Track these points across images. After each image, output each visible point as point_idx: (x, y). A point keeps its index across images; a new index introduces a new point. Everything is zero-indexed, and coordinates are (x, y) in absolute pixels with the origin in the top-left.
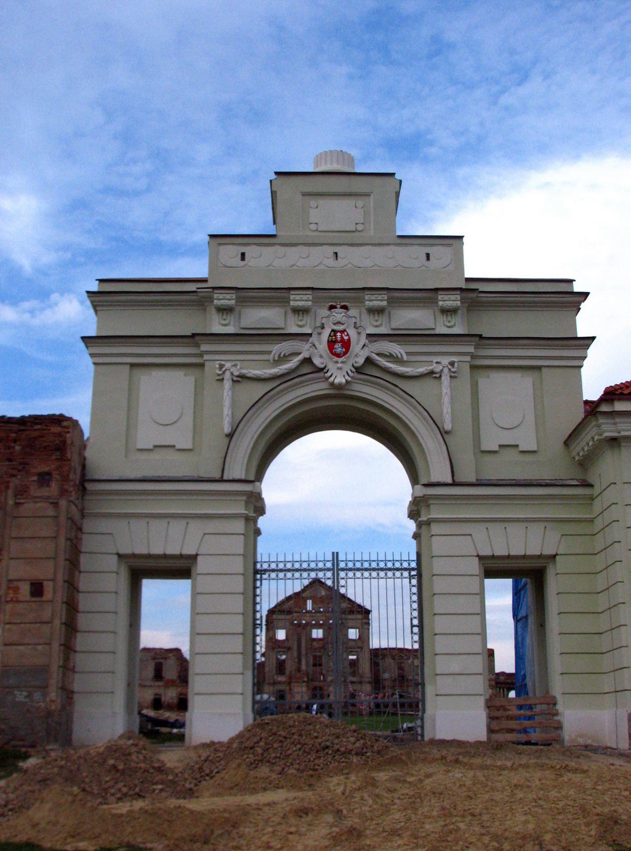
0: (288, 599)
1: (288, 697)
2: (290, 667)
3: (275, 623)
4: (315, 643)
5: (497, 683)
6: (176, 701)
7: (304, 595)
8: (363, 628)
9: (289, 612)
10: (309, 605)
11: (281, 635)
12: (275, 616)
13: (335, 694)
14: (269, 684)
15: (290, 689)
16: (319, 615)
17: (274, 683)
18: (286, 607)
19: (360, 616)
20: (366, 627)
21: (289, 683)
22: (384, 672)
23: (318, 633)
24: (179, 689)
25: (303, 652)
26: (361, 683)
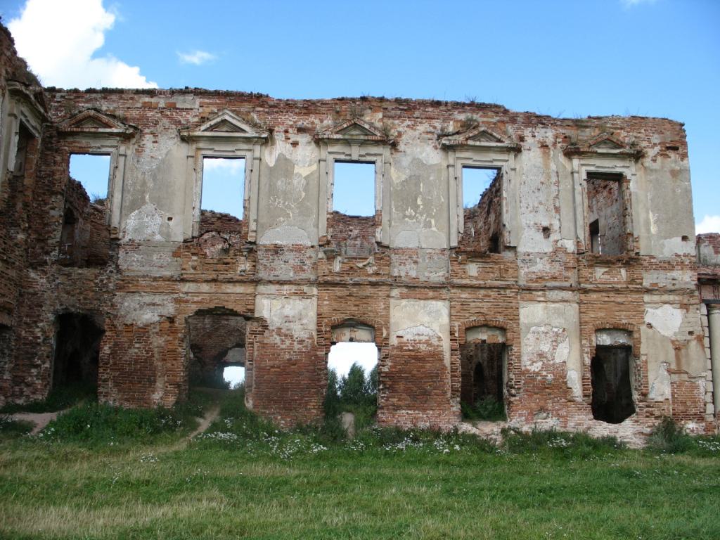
5: (703, 282)
22: (136, 204)
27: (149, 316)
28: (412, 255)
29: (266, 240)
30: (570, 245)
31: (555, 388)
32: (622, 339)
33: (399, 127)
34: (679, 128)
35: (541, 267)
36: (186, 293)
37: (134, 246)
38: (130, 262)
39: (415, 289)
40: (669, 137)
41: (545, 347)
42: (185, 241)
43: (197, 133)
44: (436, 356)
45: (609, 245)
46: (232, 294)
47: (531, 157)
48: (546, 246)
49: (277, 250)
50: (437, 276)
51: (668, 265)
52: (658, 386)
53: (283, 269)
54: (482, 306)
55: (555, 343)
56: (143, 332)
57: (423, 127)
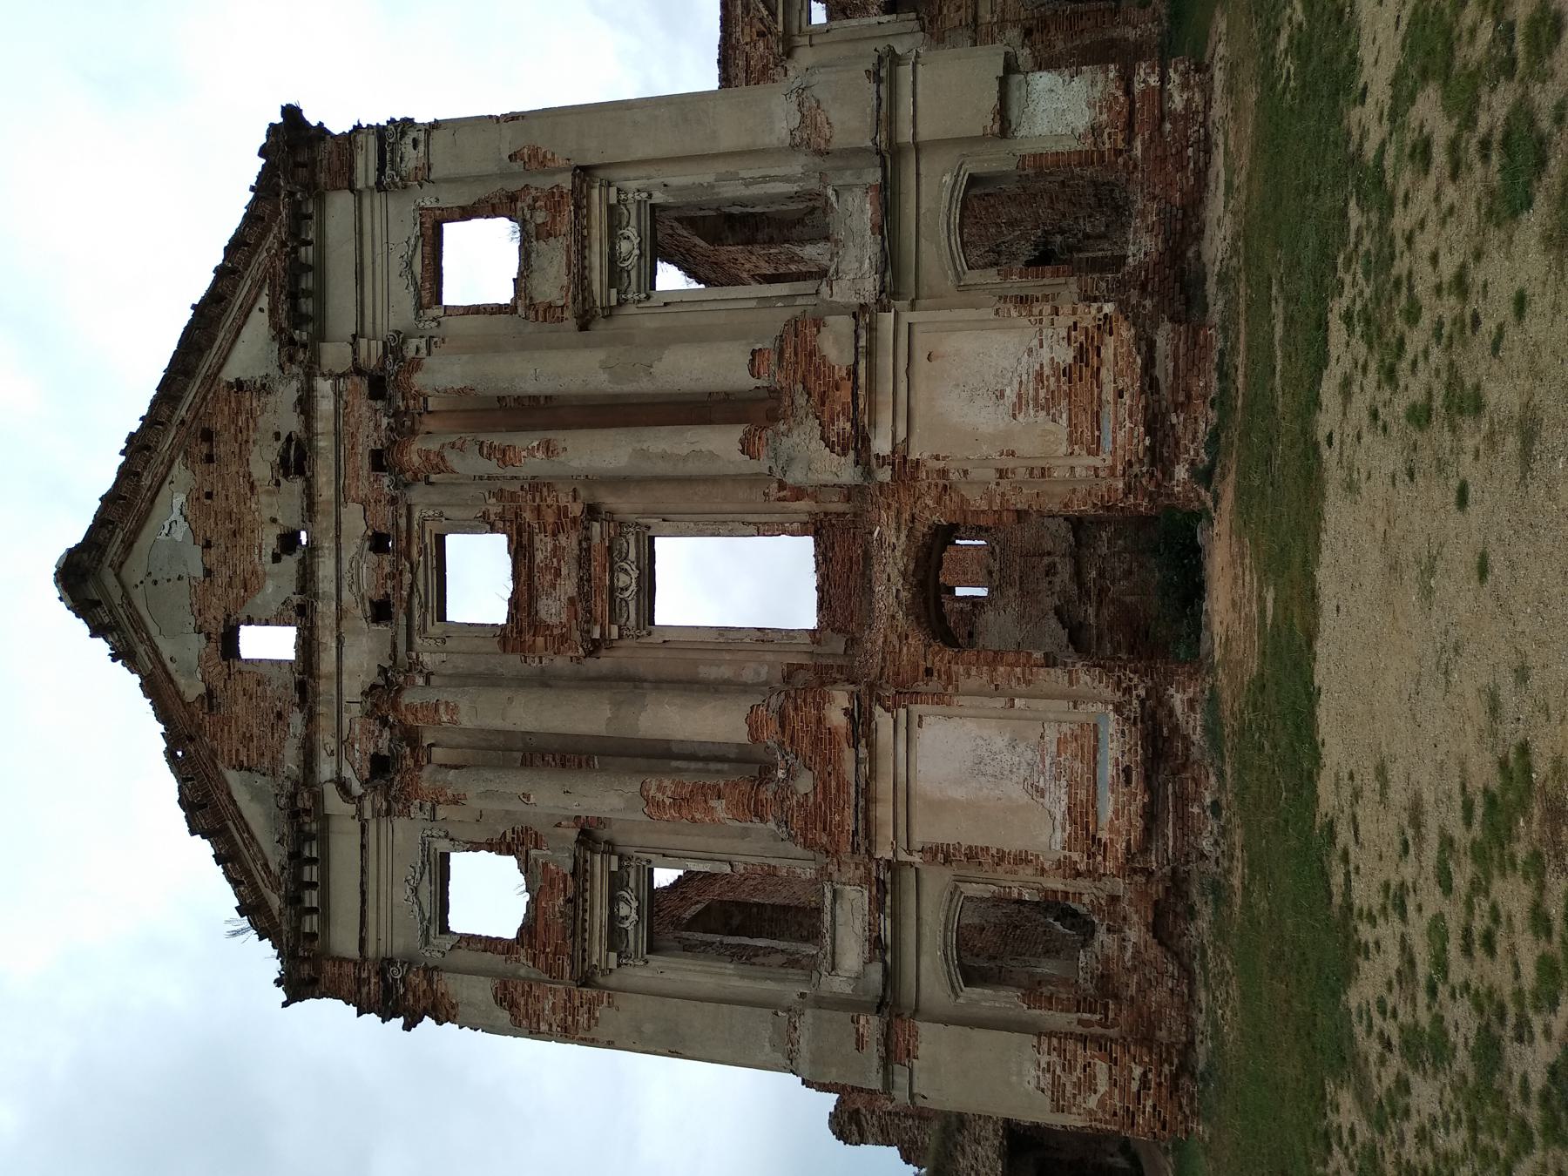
0: (205, 809)
3: (397, 934)
4: (552, 609)
7: (192, 689)
8: (425, 175)
9: (303, 820)
10: (270, 643)
11: (488, 895)
12: (344, 940)
14: (894, 1053)
15: (942, 855)
16: (326, 569)
17: (891, 1005)
19: (340, 206)
20: (411, 158)
23: (479, 579)
25: (585, 716)
26: (890, 156)
36: (992, 12)
42: (923, 30)
43: (781, 28)
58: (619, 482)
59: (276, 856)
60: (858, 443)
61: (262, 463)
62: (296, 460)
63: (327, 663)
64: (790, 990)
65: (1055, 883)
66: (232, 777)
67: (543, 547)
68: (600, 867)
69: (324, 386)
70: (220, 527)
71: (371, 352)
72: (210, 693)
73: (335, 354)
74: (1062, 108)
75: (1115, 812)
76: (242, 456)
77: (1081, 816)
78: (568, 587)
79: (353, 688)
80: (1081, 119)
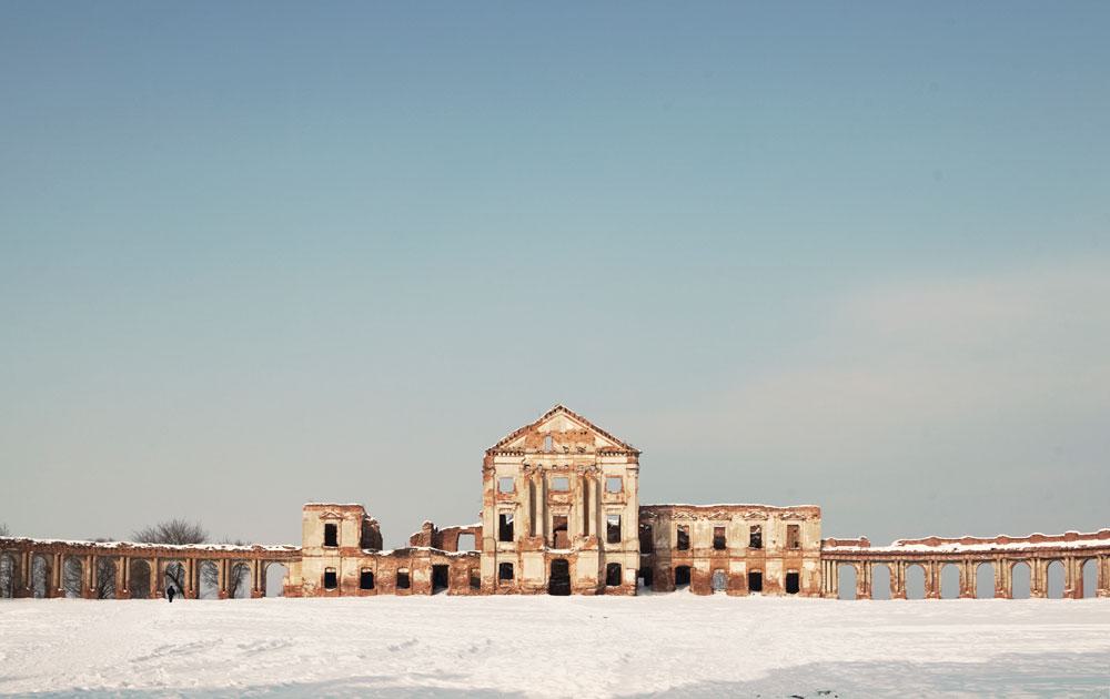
1: (516, 571)
2: (520, 531)
5: (821, 555)
6: (356, 577)
7: (540, 429)
9: (519, 452)
12: (497, 459)
13: (585, 568)
18: (514, 444)
19: (624, 459)
21: (519, 553)
24: (362, 561)
27: (666, 567)
28: (736, 550)
29: (696, 547)
30: (781, 545)
31: (774, 585)
32: (795, 571)
33: (733, 513)
34: (819, 510)
35: (772, 552)
37: (660, 549)
38: (659, 553)
39: (737, 559)
40: (815, 512)
41: (773, 573)
44: (742, 576)
45: (794, 542)
46: (687, 561)
47: (771, 520)
48: (775, 546)
49: (698, 549)
50: (743, 555)
51: (811, 551)
52: (805, 583)
53: (700, 554)
54: (755, 562)
55: (776, 571)
56: (664, 573)
57: (739, 514)
58: (576, 510)
59: (511, 446)
60: (581, 550)
61: (581, 445)
62: (582, 451)
63: (546, 456)
64: (497, 538)
65: (516, 577)
66: (524, 438)
67: (565, 496)
68: (513, 506)
69: (594, 456)
70: (570, 435)
71: (599, 466)
72: (538, 433)
73: (599, 459)
74: (629, 576)
75: (531, 584)
76: (581, 441)
77: (529, 580)
78: (559, 501)
79: (540, 462)
80: (628, 580)
